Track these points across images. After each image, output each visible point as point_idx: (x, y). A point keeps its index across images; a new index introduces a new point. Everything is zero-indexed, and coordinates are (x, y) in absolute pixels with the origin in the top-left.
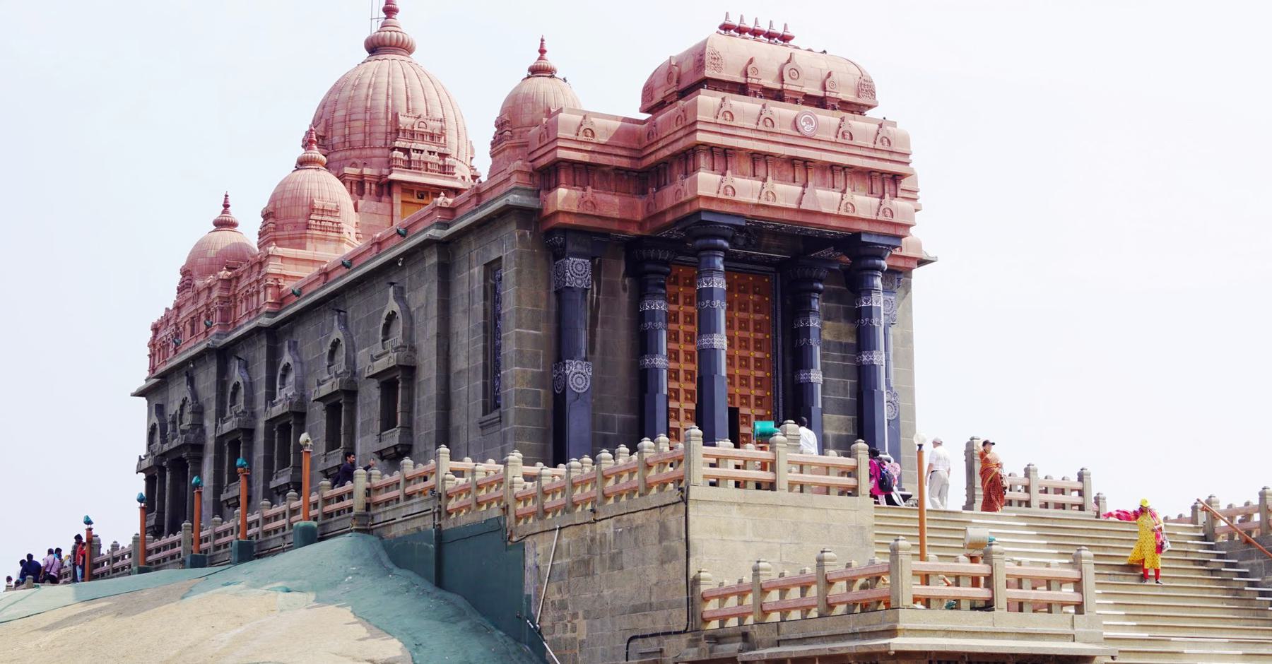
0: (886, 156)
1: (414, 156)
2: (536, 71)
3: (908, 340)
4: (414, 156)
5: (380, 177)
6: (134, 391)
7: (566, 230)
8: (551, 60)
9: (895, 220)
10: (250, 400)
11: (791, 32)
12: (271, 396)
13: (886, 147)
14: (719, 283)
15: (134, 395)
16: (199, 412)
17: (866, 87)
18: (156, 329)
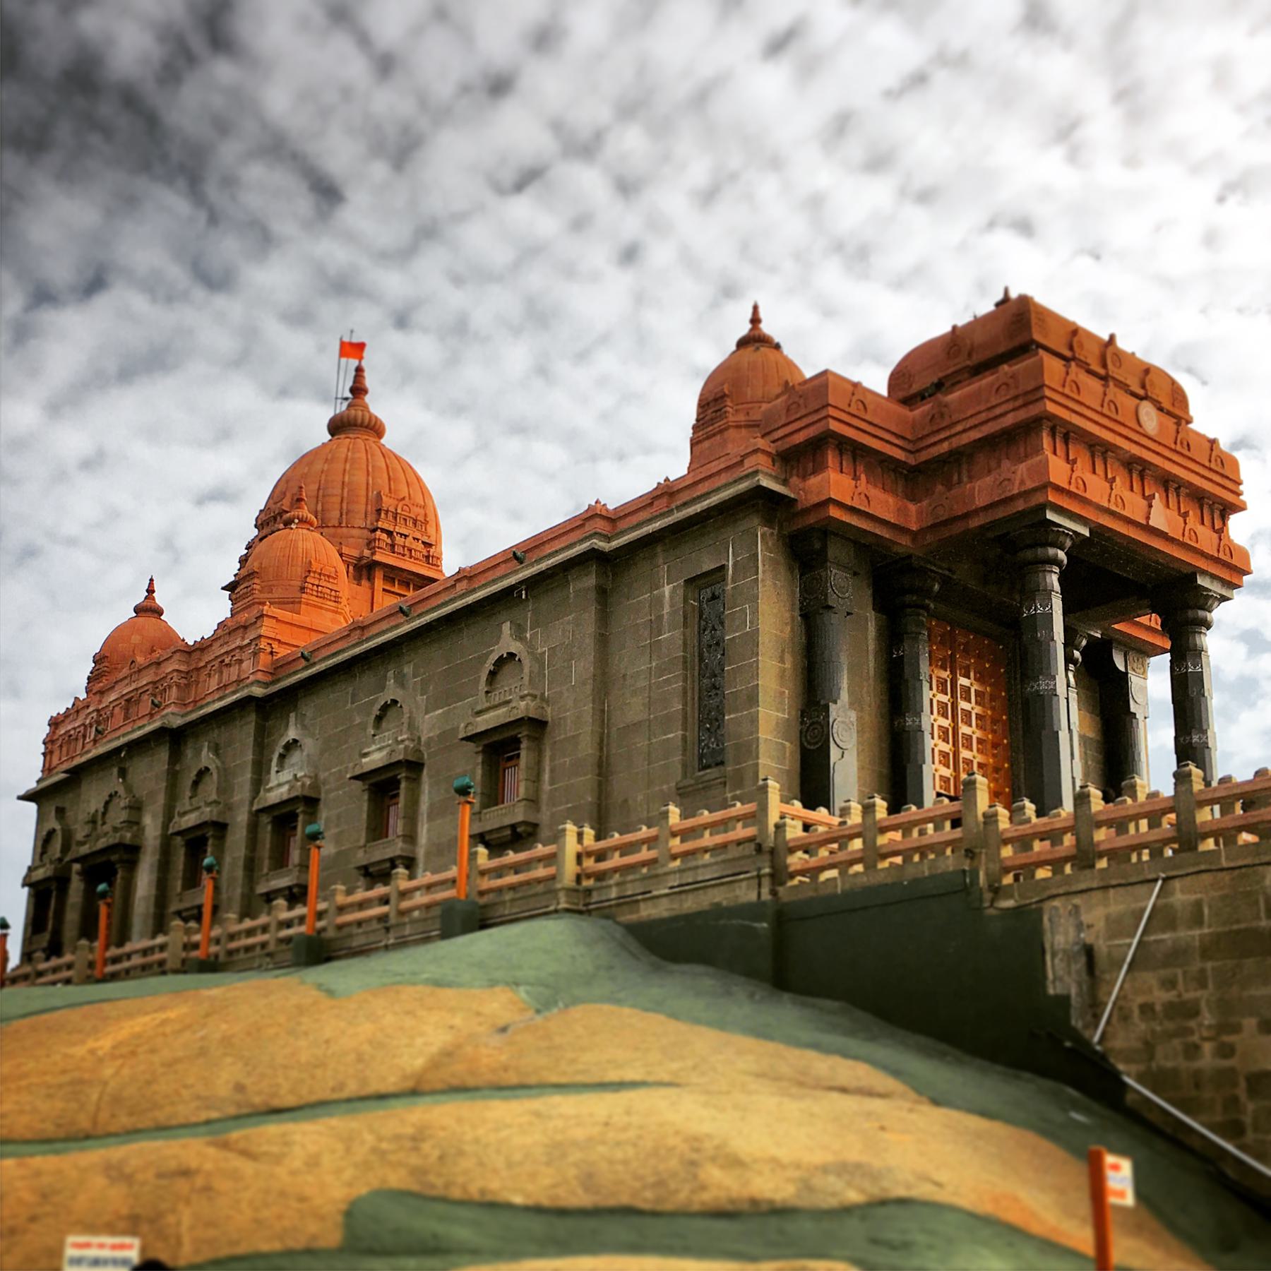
1: (399, 540)
4: (399, 540)
5: (361, 558)
6: (22, 793)
10: (225, 788)
12: (259, 782)
15: (20, 798)
16: (136, 808)
18: (55, 723)
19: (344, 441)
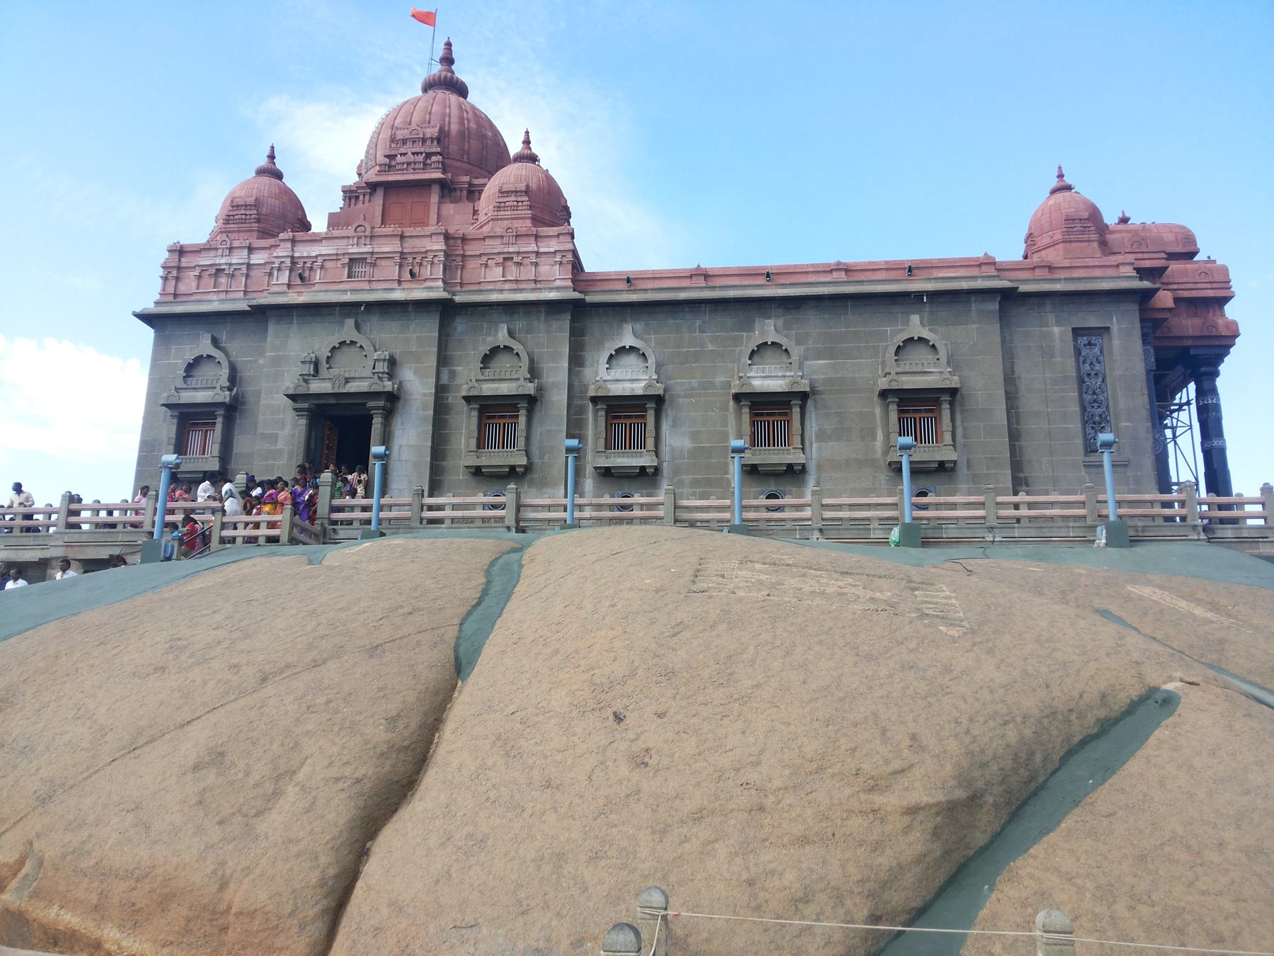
6: (138, 310)
19: (431, 92)
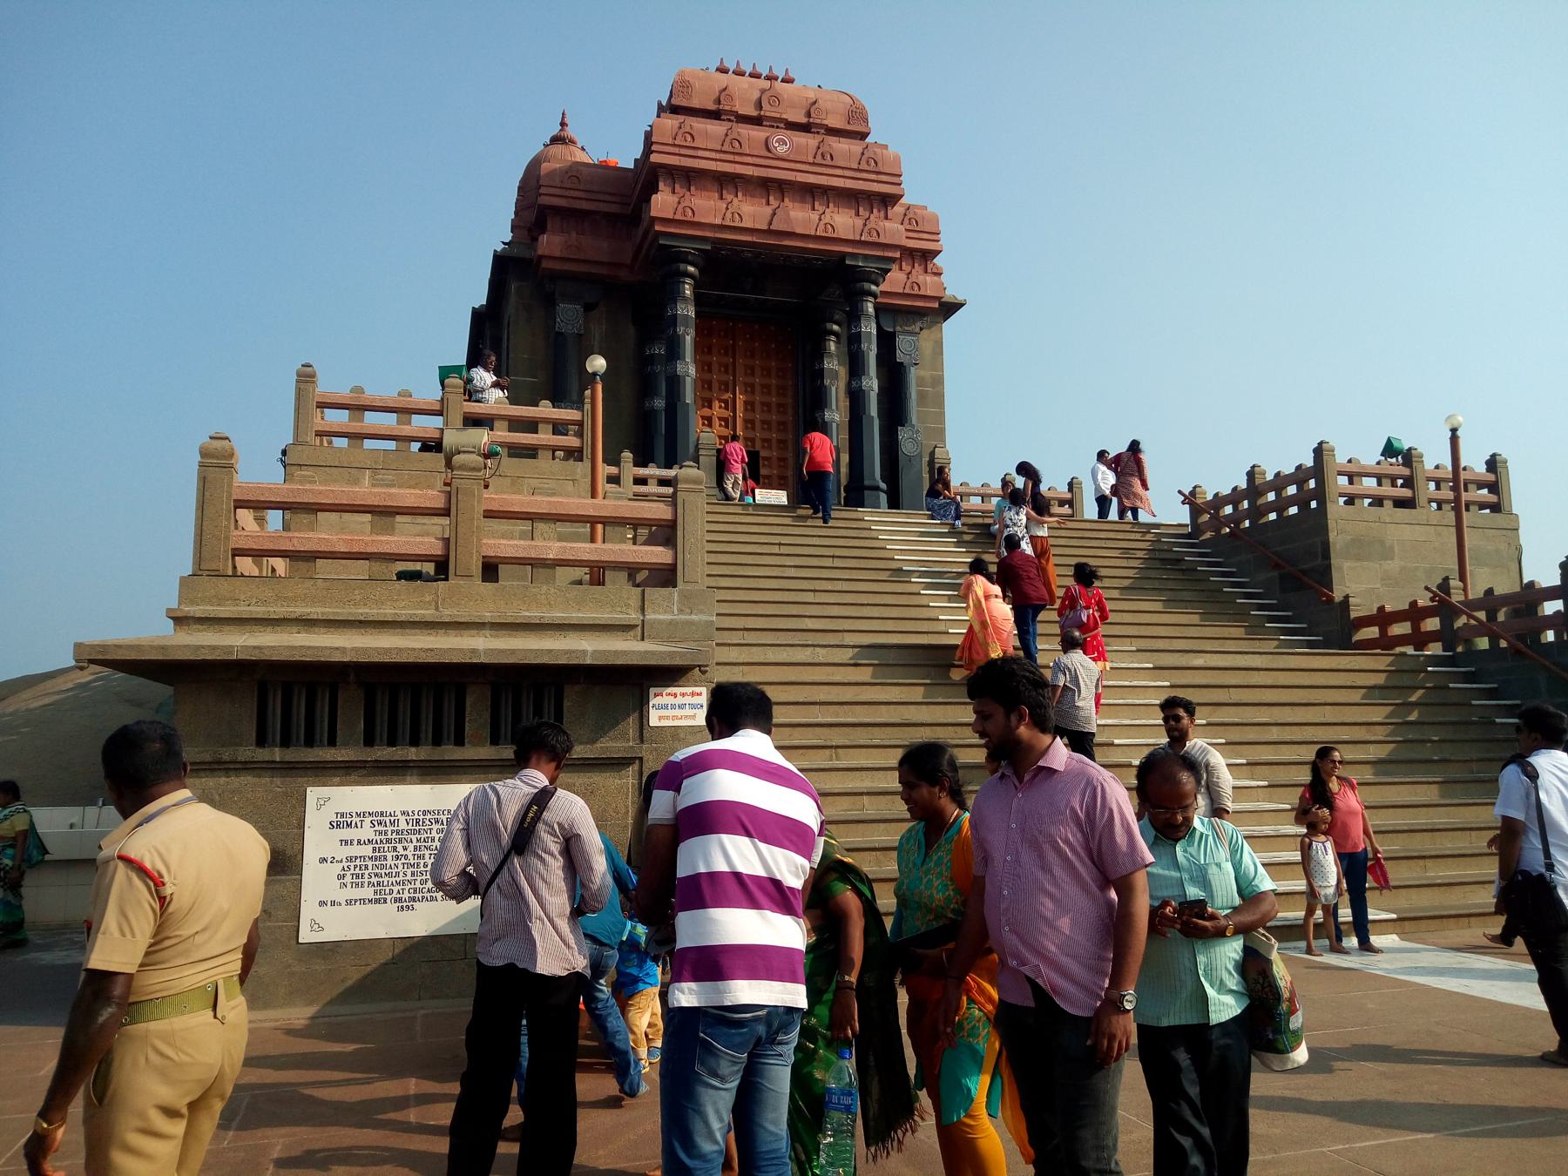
0: (873, 177)
2: (556, 140)
3: (938, 381)
7: (555, 276)
8: (570, 131)
9: (882, 240)
11: (791, 75)
13: (872, 166)
14: (687, 310)
17: (857, 113)
